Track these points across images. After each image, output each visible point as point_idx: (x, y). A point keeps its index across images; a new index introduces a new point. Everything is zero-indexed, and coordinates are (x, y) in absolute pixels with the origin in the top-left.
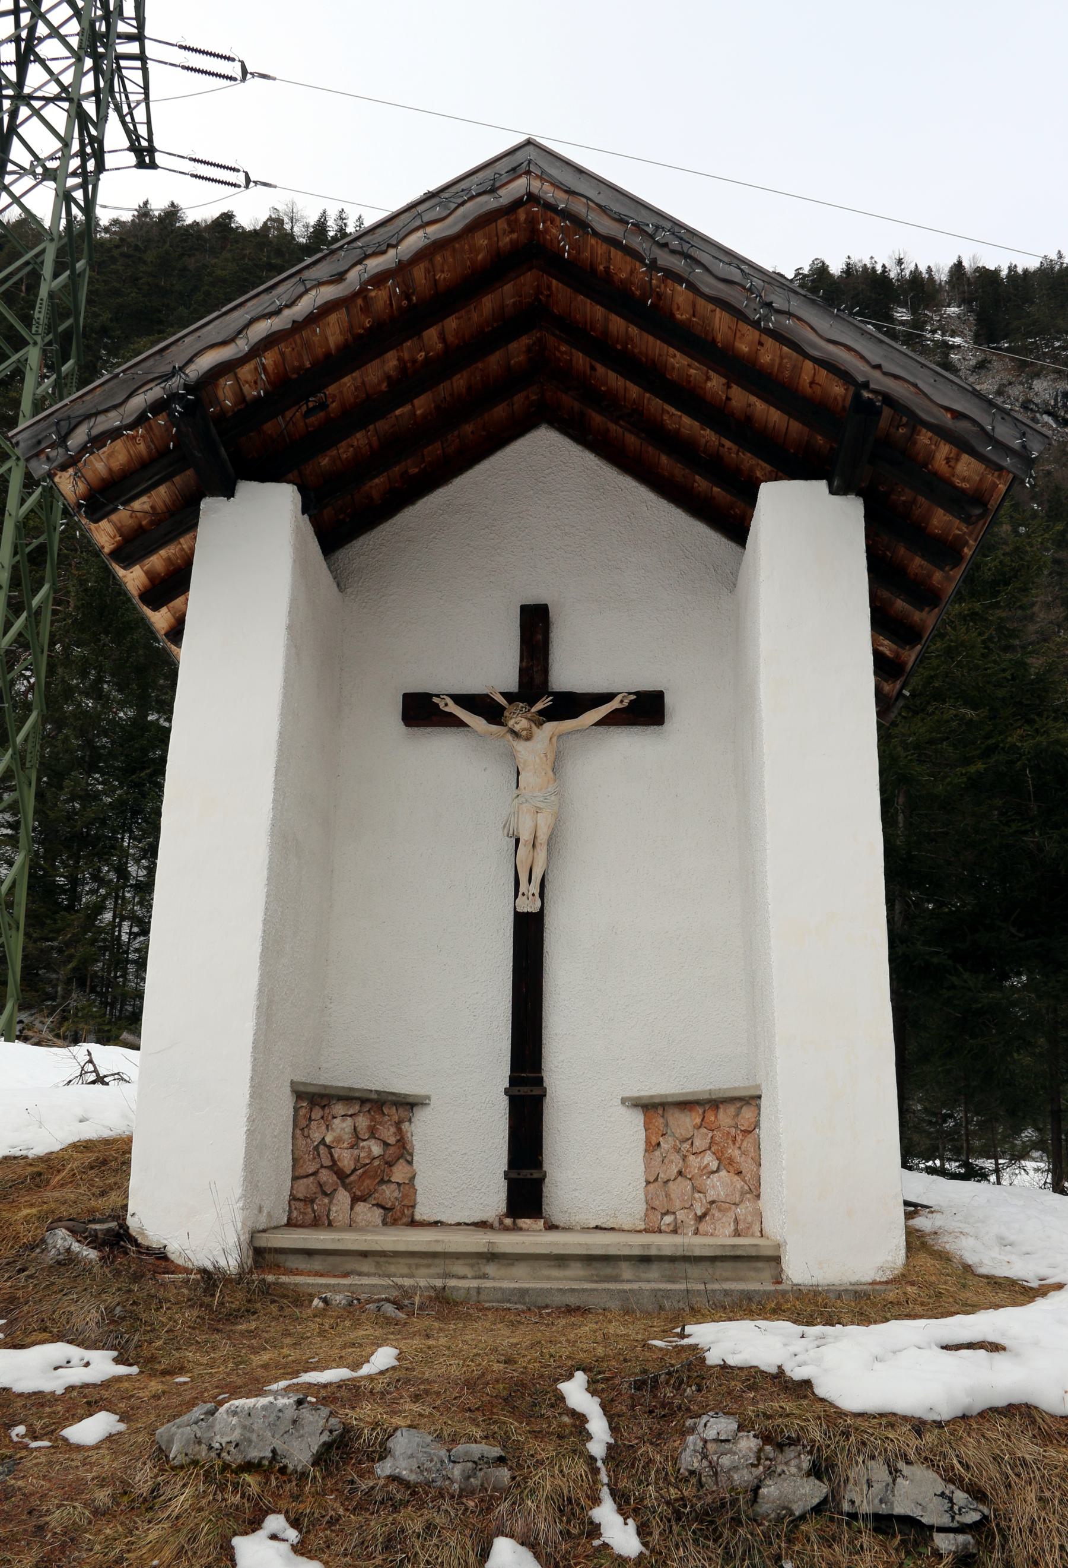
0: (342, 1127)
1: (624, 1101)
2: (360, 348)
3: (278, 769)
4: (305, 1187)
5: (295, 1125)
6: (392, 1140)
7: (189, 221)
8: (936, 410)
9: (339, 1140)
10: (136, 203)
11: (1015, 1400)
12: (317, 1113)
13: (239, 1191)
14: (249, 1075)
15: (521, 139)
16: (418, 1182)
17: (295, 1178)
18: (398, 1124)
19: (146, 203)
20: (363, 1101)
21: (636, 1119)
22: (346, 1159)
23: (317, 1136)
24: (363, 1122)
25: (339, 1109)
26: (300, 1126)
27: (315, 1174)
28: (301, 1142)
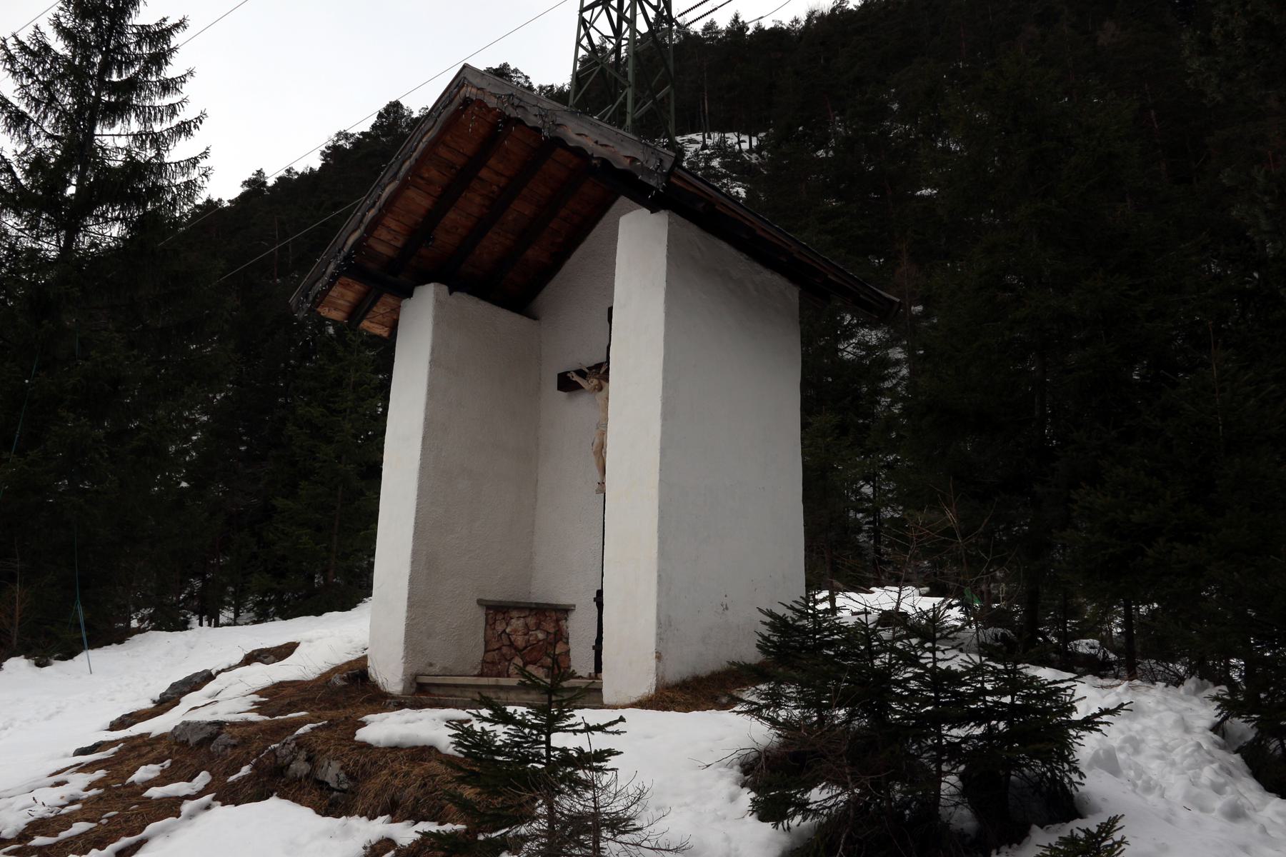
0: (517, 623)
1: (480, 602)
2: (446, 199)
3: (424, 438)
4: (490, 656)
5: (487, 623)
6: (552, 631)
7: (223, 187)
8: (345, 234)
9: (515, 631)
10: (285, 165)
11: (428, 744)
12: (500, 617)
13: (402, 654)
14: (406, 596)
15: (460, 66)
16: (572, 654)
17: (486, 651)
18: (557, 621)
19: (260, 172)
20: (531, 609)
21: (480, 614)
22: (520, 641)
23: (499, 628)
24: (531, 621)
25: (515, 614)
26: (490, 624)
27: (499, 649)
28: (490, 632)
